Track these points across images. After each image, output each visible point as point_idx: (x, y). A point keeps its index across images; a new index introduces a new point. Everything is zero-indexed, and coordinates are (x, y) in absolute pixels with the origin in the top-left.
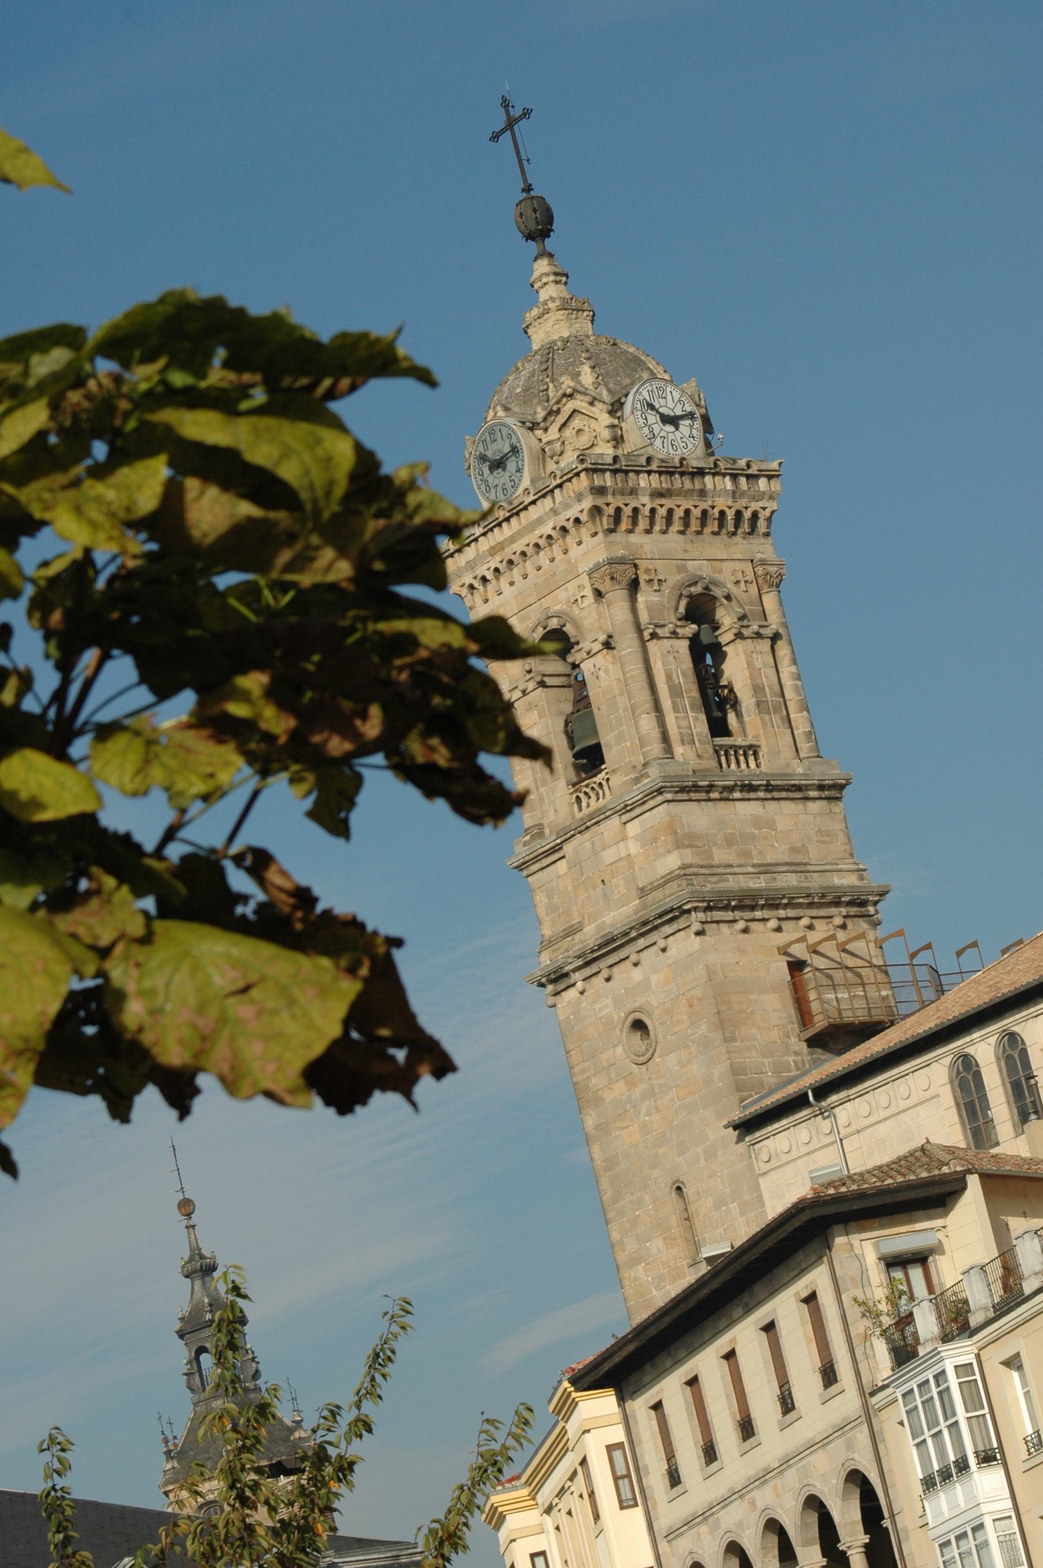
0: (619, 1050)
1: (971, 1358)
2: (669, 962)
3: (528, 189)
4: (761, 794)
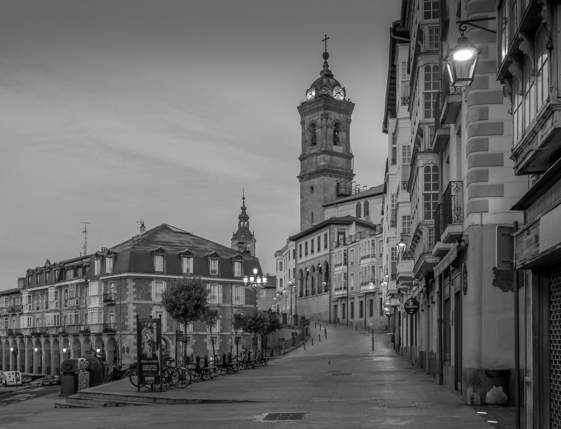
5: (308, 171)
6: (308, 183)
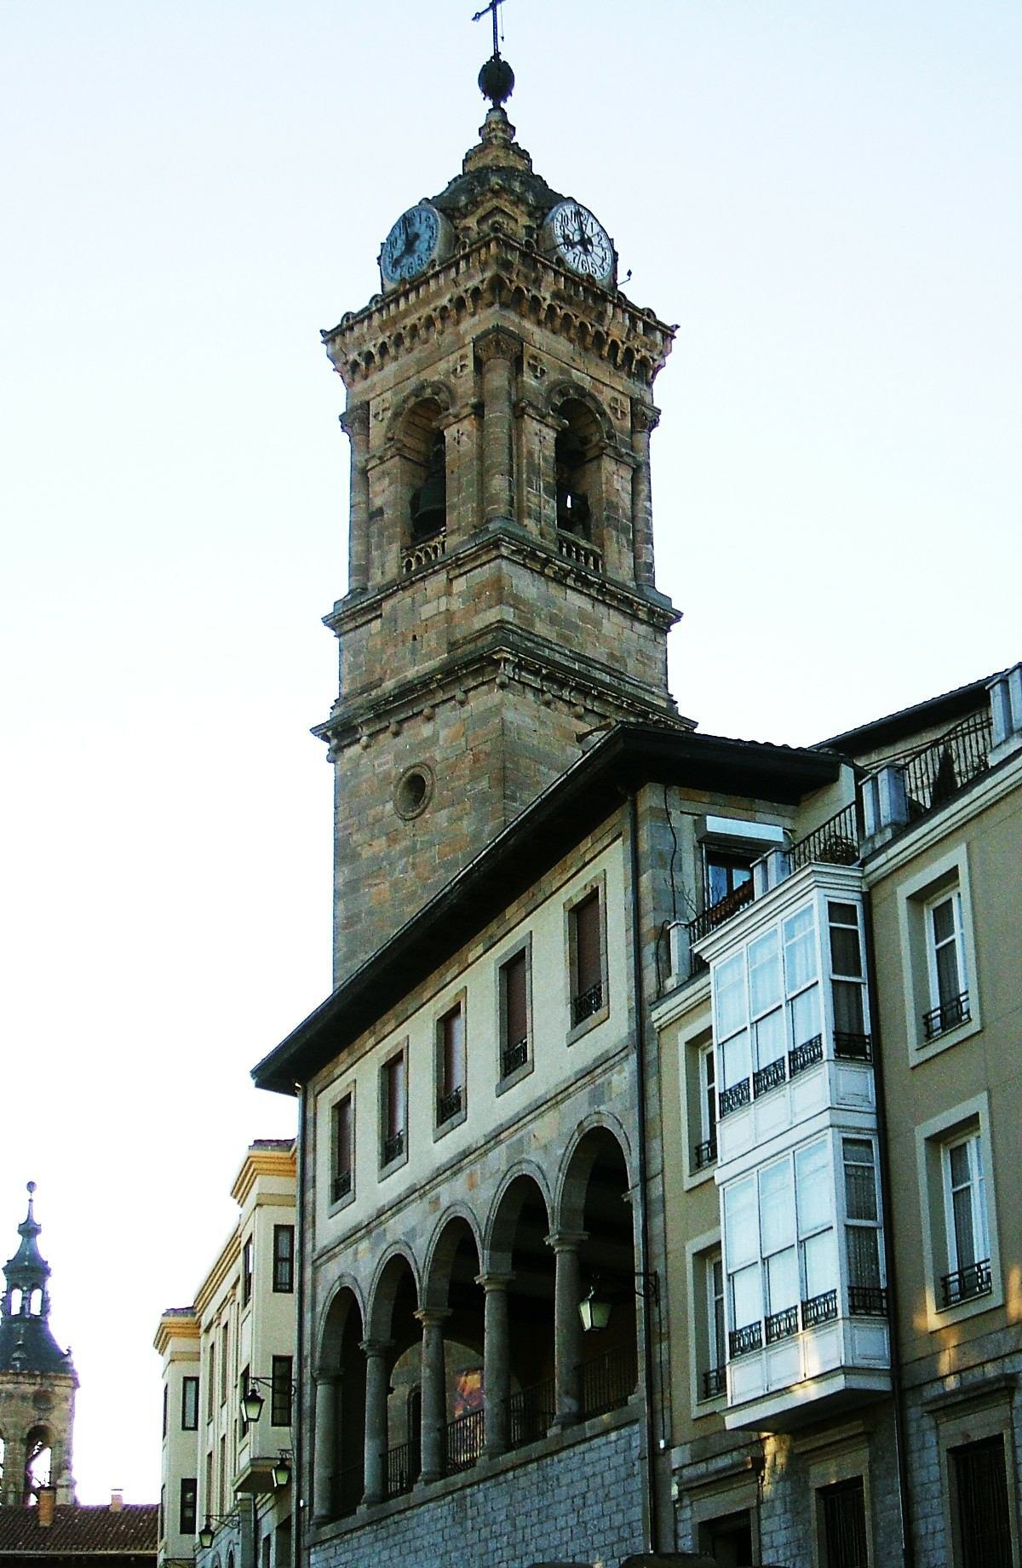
0: (389, 806)
2: (464, 716)
3: (497, 54)
4: (594, 593)
5: (389, 685)
6: (386, 758)
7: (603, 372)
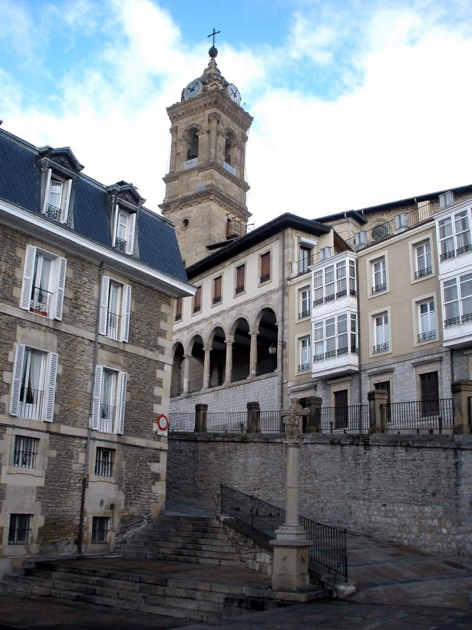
1: (354, 260)
3: (214, 46)
5: (180, 196)
7: (237, 127)
